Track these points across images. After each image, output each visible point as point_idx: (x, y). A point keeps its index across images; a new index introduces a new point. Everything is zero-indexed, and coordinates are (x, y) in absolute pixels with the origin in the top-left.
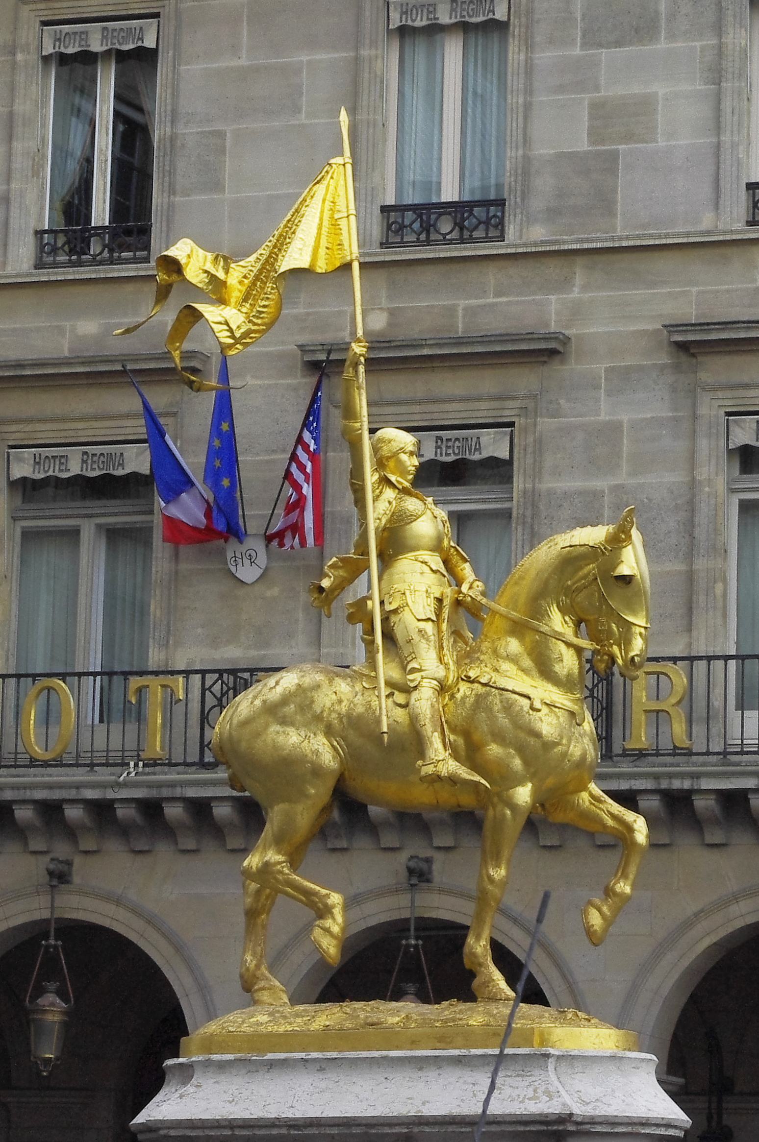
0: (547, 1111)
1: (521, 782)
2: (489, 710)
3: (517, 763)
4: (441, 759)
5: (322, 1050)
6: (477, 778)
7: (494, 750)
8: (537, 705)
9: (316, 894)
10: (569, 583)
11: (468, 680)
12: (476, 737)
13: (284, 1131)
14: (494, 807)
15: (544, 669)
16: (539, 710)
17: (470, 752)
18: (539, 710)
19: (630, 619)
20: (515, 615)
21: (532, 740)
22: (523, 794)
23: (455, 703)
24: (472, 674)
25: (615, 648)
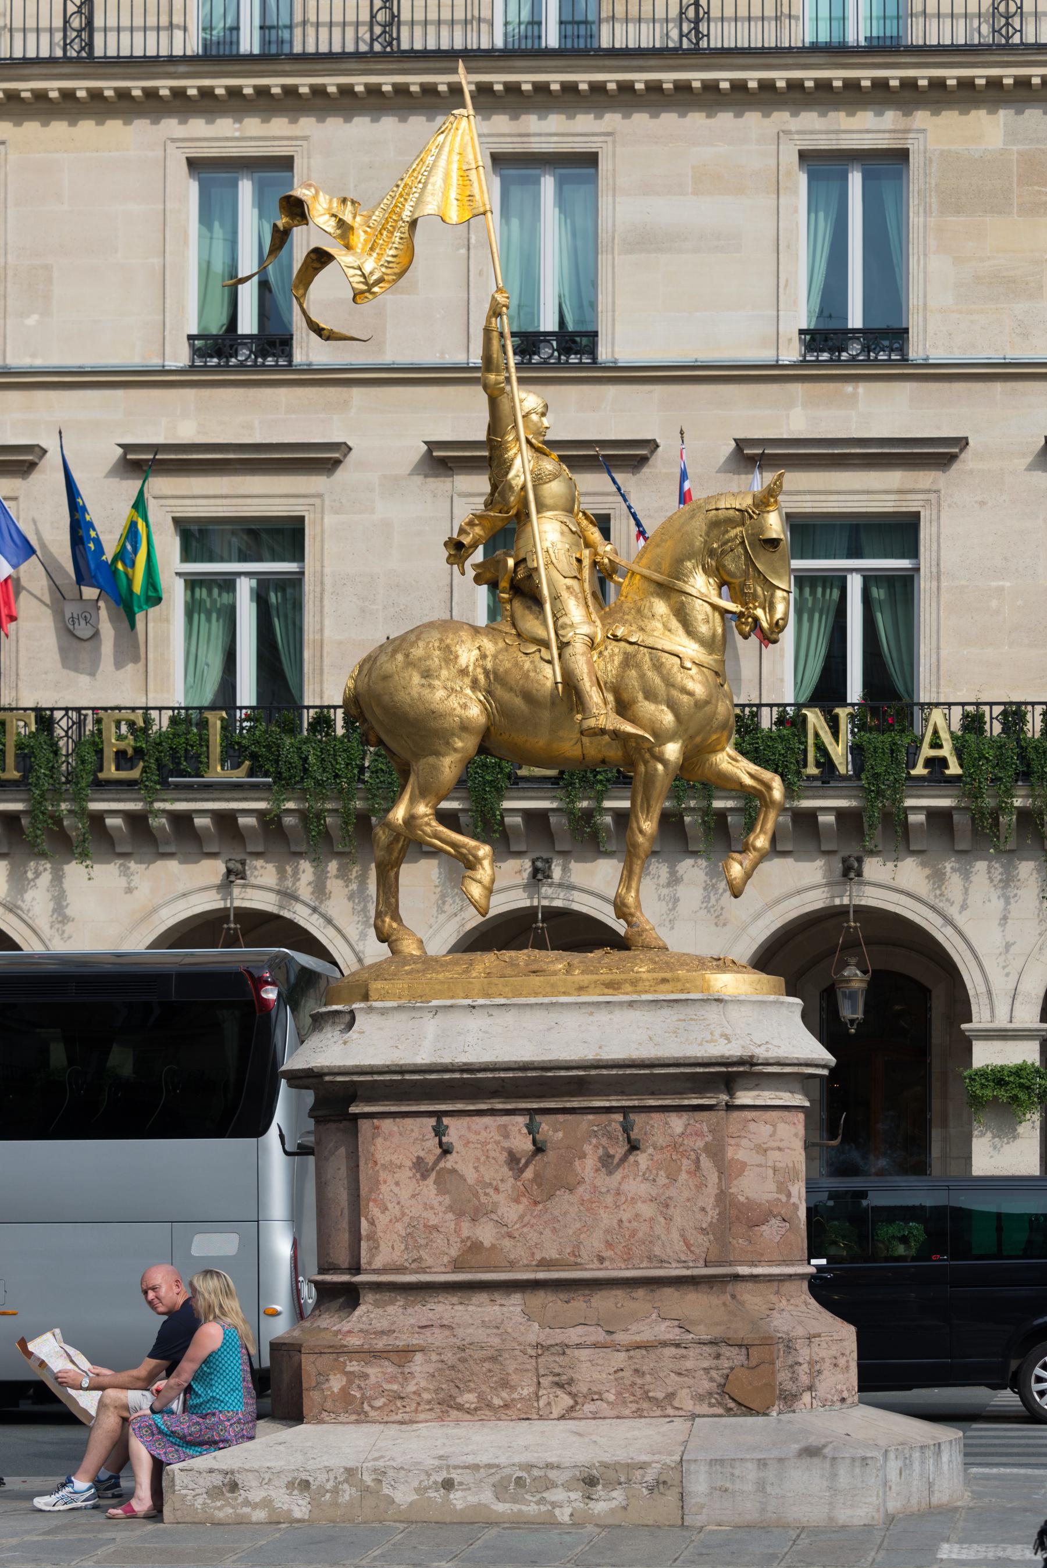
0: (727, 1054)
1: (671, 738)
2: (638, 666)
3: (668, 718)
4: (601, 712)
5: (488, 996)
6: (640, 732)
7: (647, 708)
8: (688, 664)
9: (464, 846)
10: (715, 545)
11: (616, 638)
12: (625, 696)
13: (457, 1075)
14: (646, 763)
15: (690, 630)
16: (690, 669)
17: (623, 707)
18: (690, 669)
19: (776, 583)
20: (656, 576)
21: (685, 698)
22: (672, 750)
23: (604, 660)
24: (619, 633)
25: (759, 612)
